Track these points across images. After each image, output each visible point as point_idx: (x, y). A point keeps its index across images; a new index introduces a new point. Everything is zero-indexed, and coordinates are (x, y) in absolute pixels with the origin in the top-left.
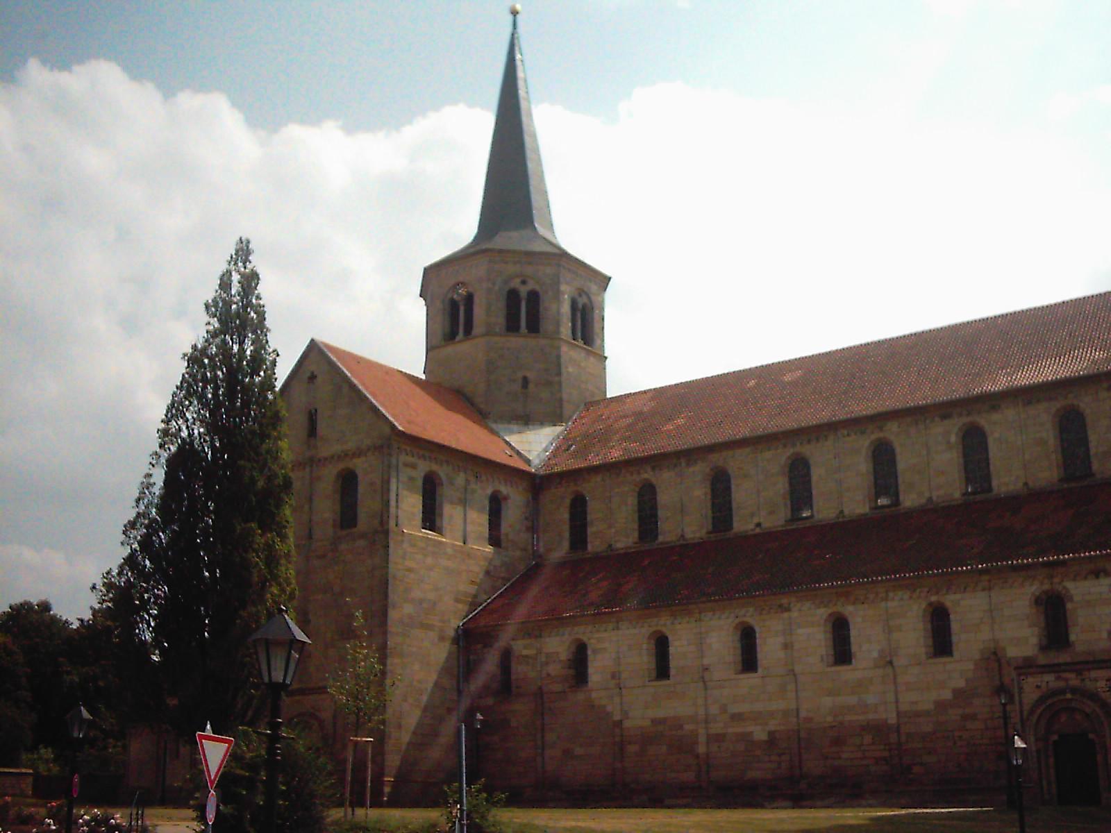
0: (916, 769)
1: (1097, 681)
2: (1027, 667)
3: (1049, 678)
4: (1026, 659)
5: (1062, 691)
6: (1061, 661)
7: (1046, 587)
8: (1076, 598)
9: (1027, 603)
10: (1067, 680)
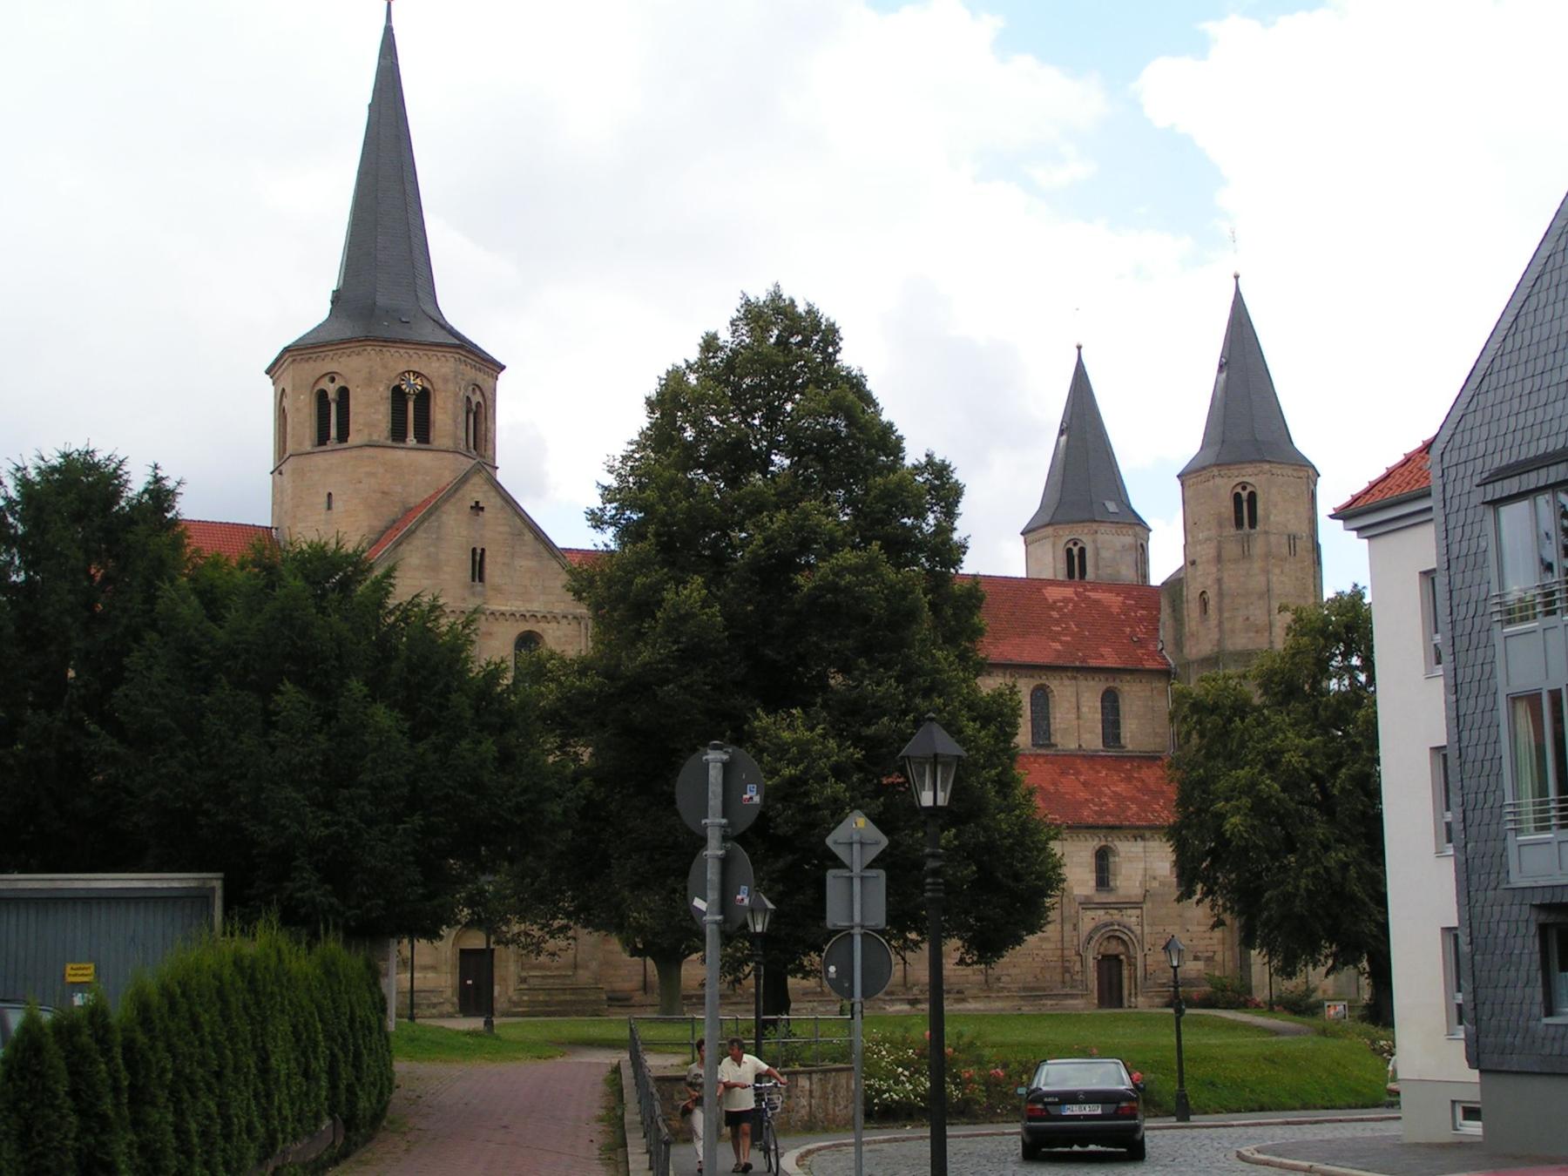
0: (1003, 979)
1: (1131, 917)
2: (1087, 904)
3: (1101, 912)
4: (1087, 897)
5: (1112, 924)
6: (1109, 901)
7: (1103, 843)
8: (1122, 854)
9: (1090, 854)
10: (1112, 915)
